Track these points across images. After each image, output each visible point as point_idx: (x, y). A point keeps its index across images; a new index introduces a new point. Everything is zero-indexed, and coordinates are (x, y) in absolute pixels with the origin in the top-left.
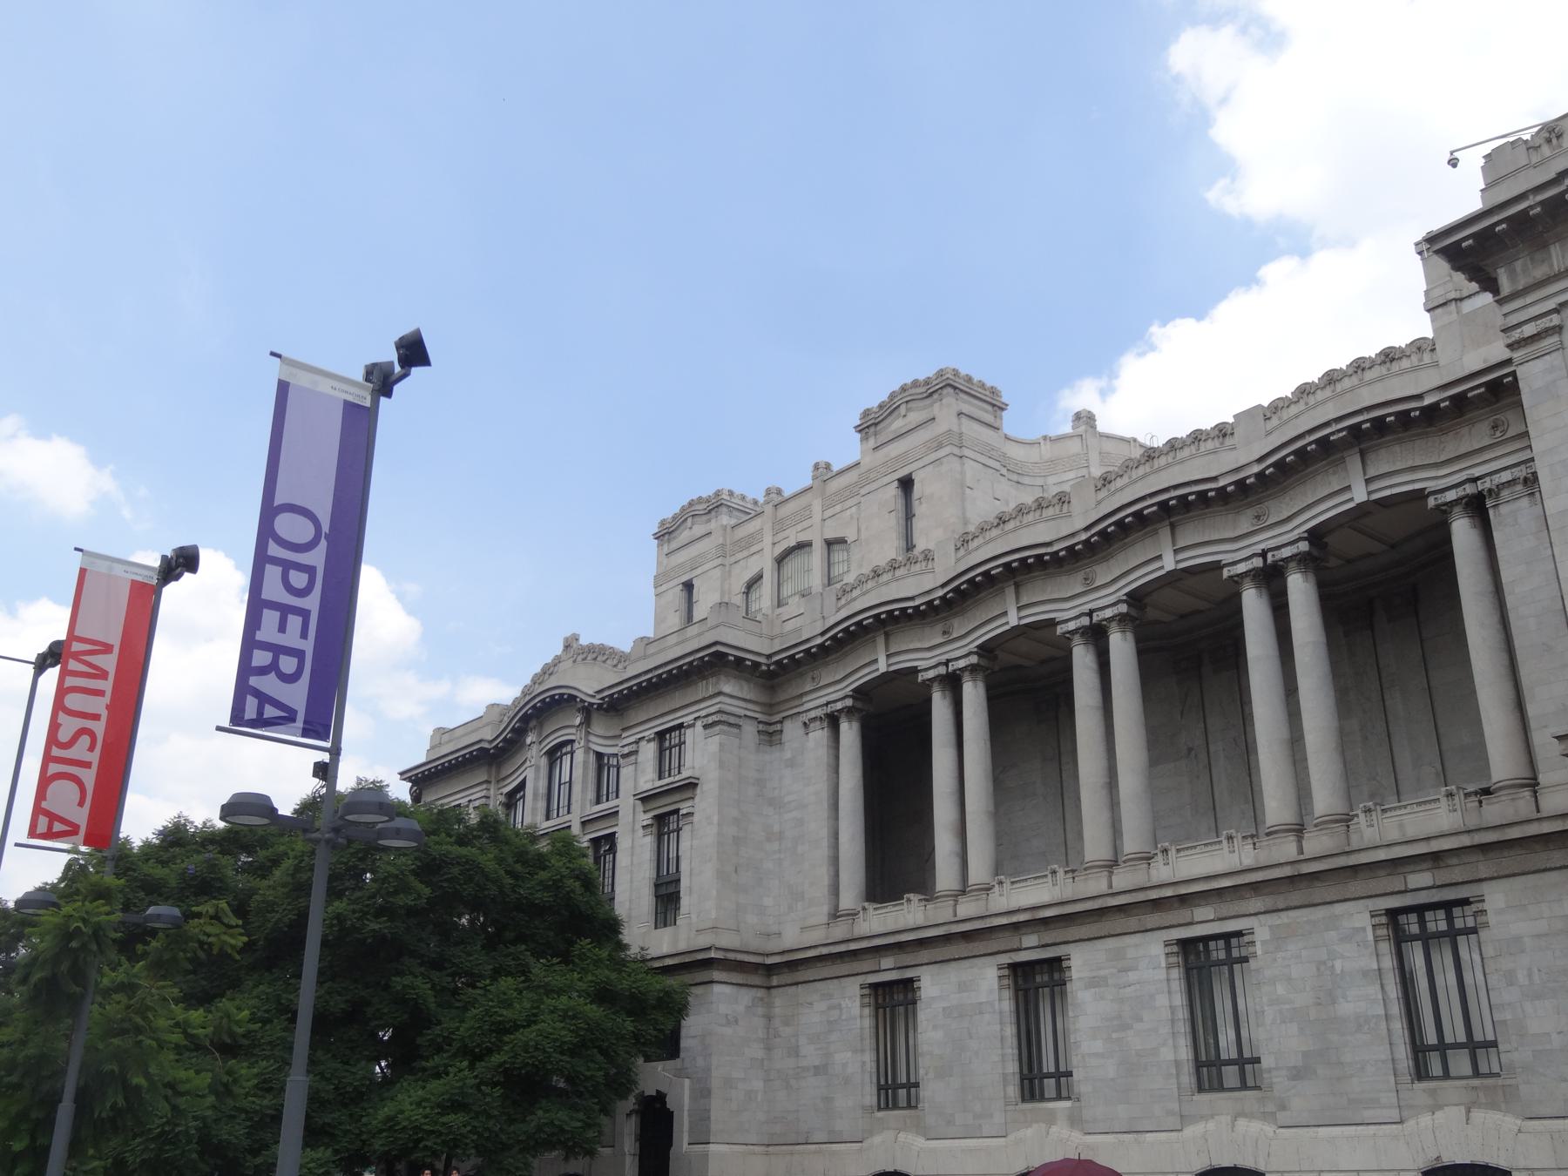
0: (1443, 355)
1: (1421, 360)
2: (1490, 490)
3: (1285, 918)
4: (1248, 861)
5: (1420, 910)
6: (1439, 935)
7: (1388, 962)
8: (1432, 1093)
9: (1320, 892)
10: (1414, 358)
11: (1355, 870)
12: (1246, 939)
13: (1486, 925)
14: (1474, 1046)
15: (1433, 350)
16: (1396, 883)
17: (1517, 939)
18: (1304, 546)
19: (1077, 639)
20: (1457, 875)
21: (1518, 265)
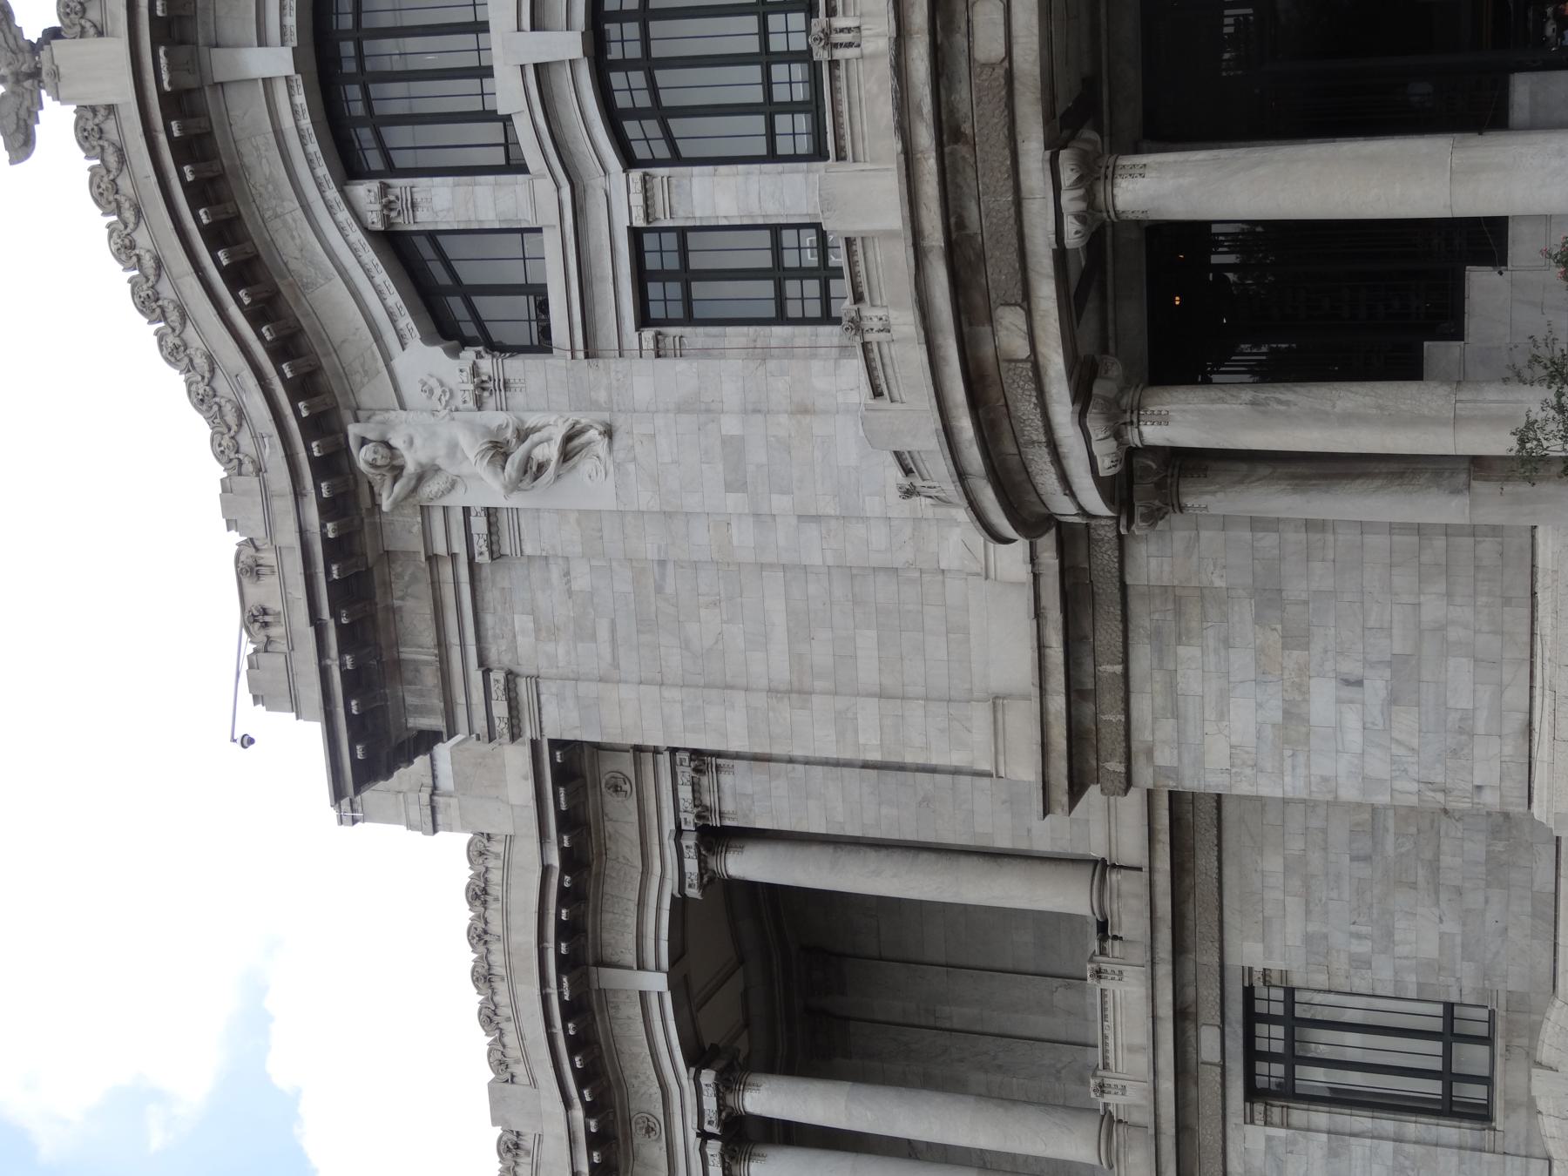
0: (500, 825)
1: (497, 856)
2: (698, 816)
5: (1252, 1055)
6: (1290, 1039)
7: (1321, 1117)
8: (1511, 1106)
10: (491, 863)
13: (1284, 974)
14: (1449, 1034)
15: (489, 837)
16: (1211, 1077)
17: (1308, 939)
18: (708, 1077)
20: (1210, 994)
21: (411, 700)
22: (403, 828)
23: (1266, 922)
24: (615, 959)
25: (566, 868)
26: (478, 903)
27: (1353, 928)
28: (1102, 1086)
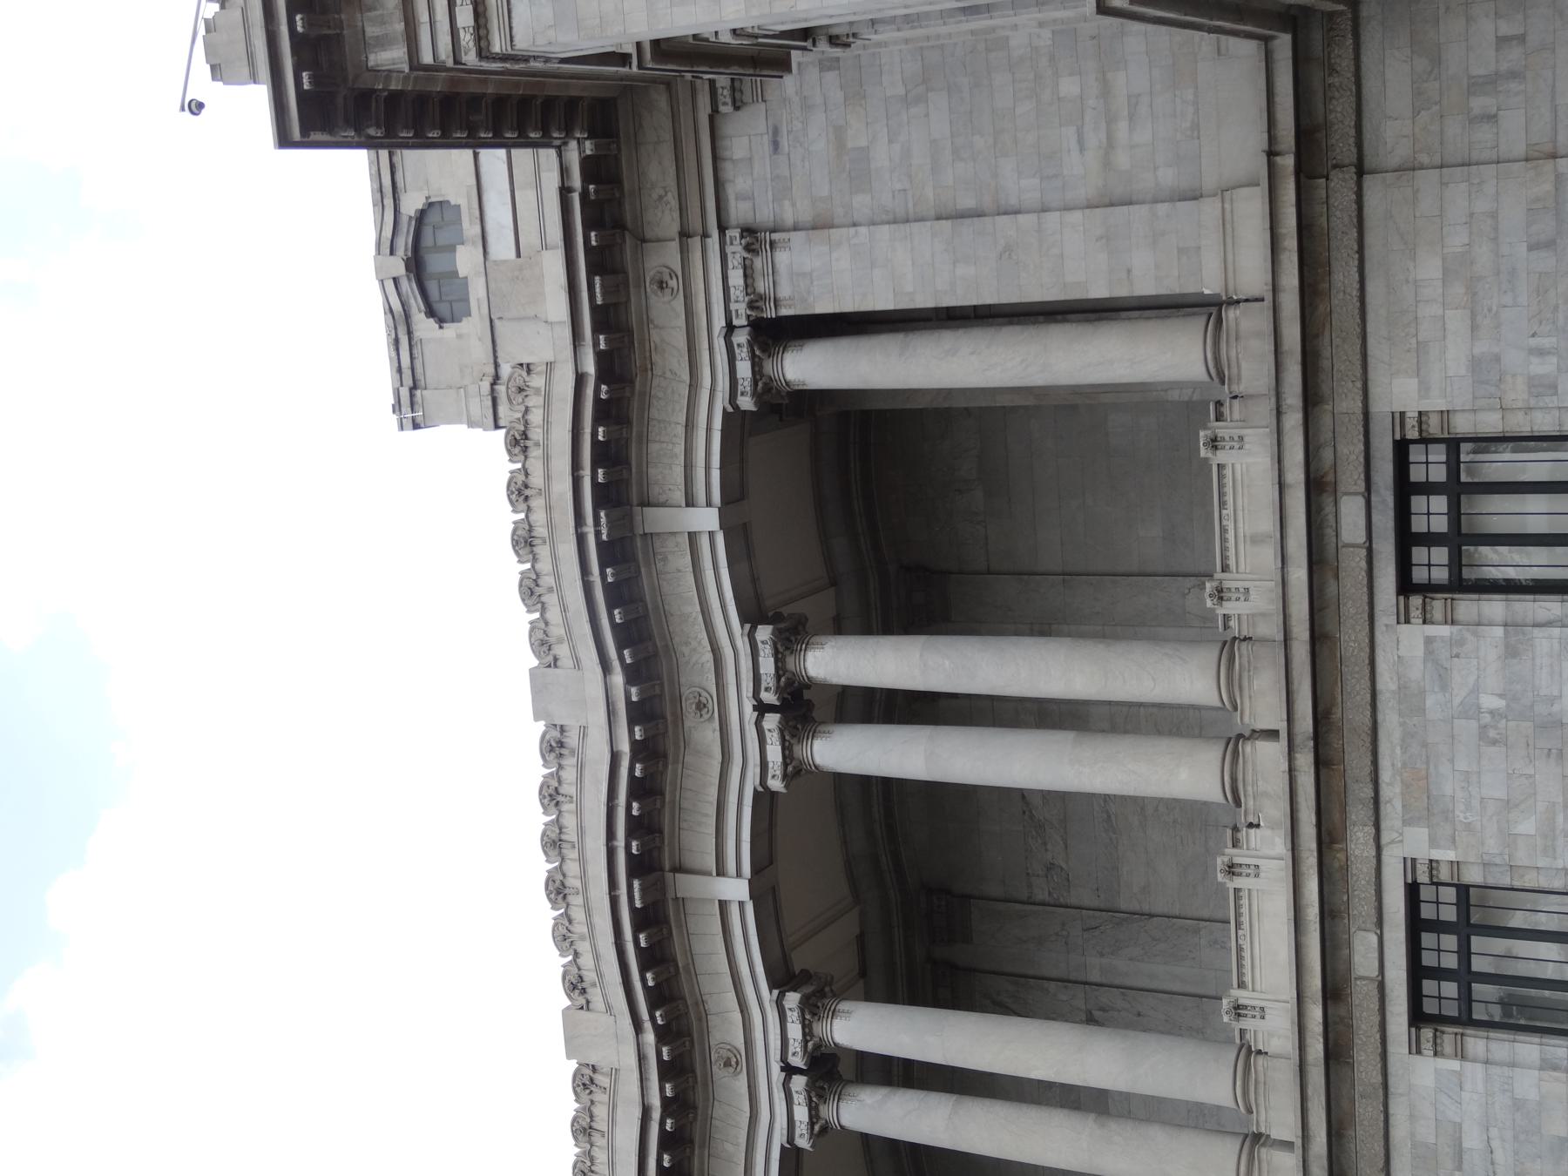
1: (537, 391)
2: (751, 306)
3: (1391, 791)
4: (1280, 846)
5: (1406, 539)
6: (1455, 513)
7: (1494, 607)
9: (1353, 713)
10: (531, 402)
11: (1318, 638)
12: (1423, 878)
13: (1445, 415)
15: (529, 368)
16: (1354, 563)
17: (1475, 364)
19: (827, 1112)
21: (372, 31)
22: (465, 426)
23: (1421, 348)
24: (662, 499)
25: (602, 377)
26: (517, 450)
27: (1533, 342)
28: (1220, 590)
